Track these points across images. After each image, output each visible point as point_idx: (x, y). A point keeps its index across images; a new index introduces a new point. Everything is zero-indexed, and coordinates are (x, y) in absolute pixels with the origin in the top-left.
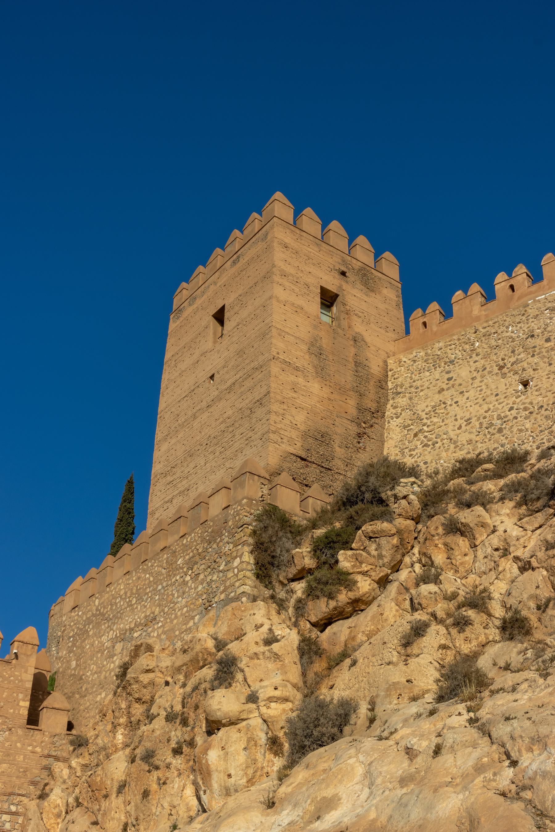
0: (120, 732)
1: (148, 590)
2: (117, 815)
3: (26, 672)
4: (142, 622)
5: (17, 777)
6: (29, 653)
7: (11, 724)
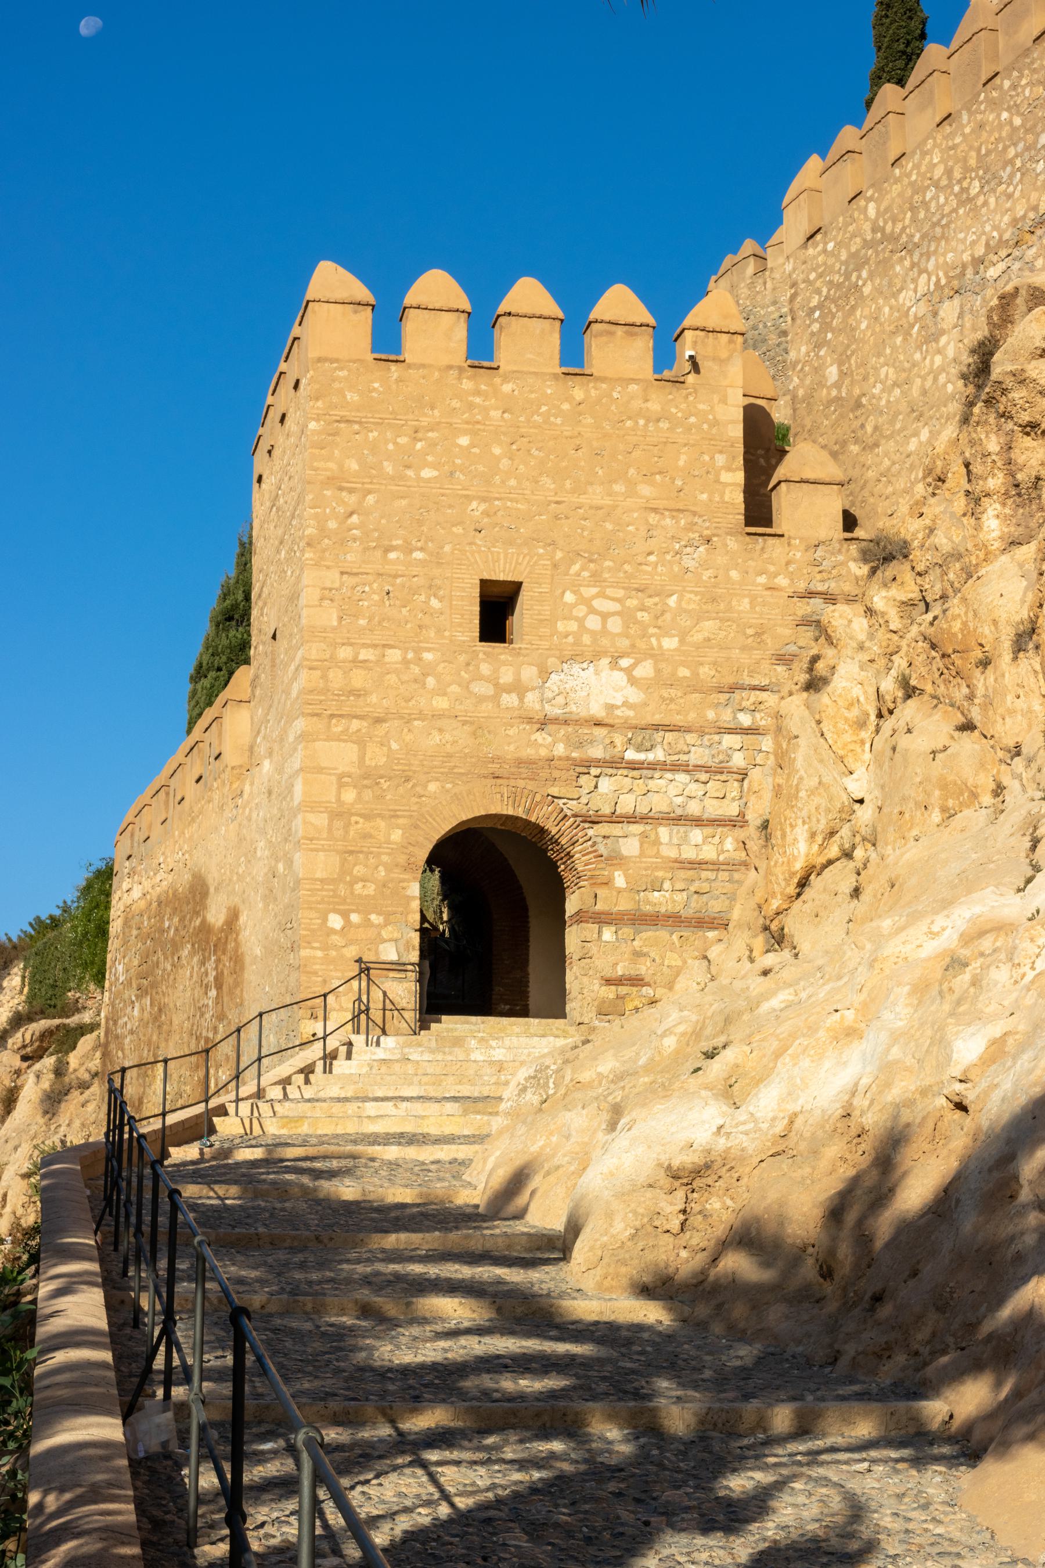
0: (991, 512)
1: (1012, 152)
2: (1020, 704)
3: (724, 401)
4: (1007, 236)
5: (743, 648)
6: (724, 354)
7: (707, 528)
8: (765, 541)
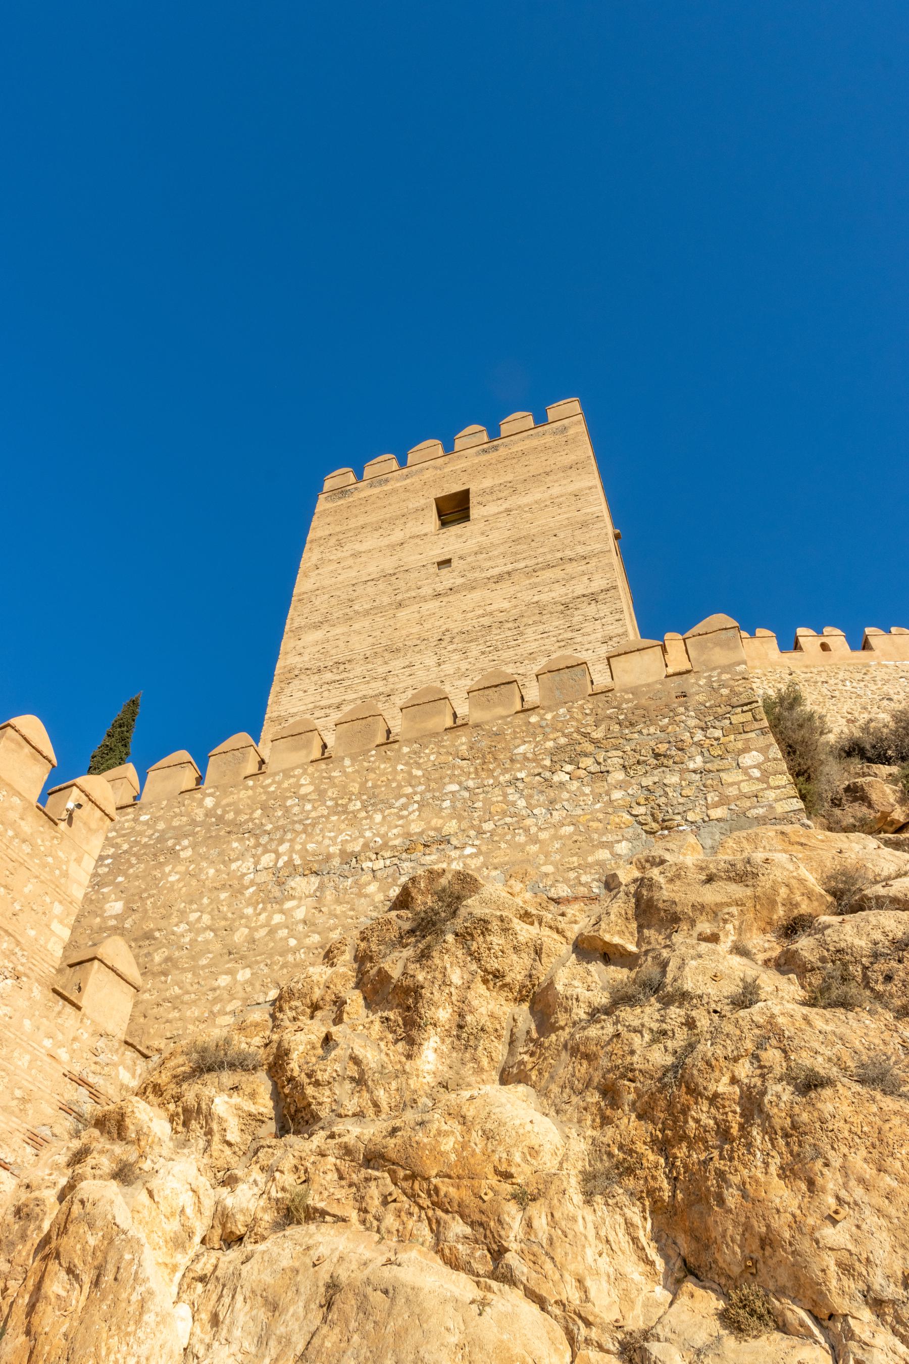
3: (79, 861)
6: (93, 825)
7: (22, 965)
8: (64, 1006)
